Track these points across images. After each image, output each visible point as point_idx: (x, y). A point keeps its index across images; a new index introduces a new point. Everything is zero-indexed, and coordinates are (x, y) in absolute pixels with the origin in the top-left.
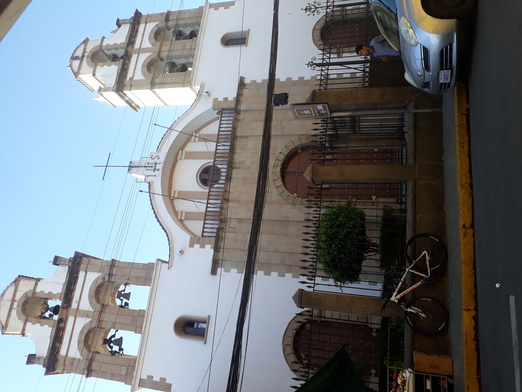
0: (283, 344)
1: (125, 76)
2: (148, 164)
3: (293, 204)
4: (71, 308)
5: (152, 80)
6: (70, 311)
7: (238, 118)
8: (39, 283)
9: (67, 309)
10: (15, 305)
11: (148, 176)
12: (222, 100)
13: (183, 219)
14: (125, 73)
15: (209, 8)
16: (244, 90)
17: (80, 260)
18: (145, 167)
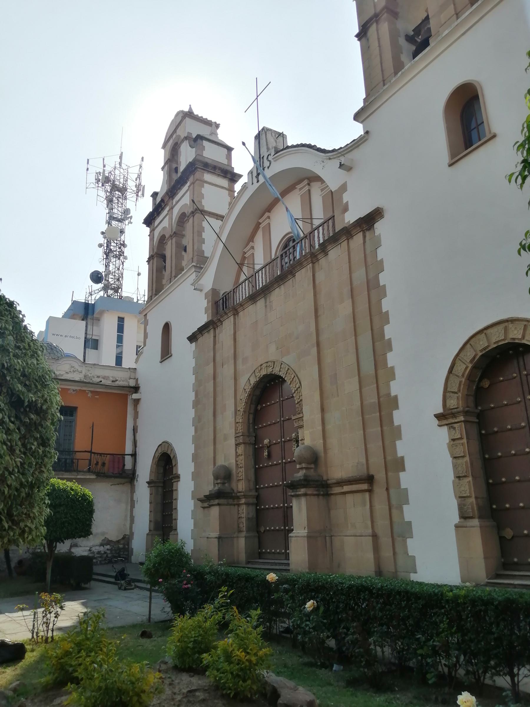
7: (319, 256)
9: (169, 198)
12: (345, 202)
13: (246, 255)
16: (361, 233)
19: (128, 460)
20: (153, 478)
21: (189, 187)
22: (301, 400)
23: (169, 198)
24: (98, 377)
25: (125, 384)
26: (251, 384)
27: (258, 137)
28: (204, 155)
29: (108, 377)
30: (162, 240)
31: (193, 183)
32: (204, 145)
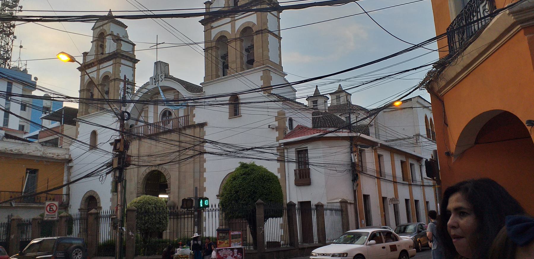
0: (90, 191)
1: (213, 21)
2: (158, 75)
3: (138, 183)
4: (100, 65)
5: (210, 48)
6: (98, 66)
8: (109, 36)
9: (98, 63)
10: (101, 28)
11: (152, 79)
12: (194, 113)
14: (215, 19)
15: (263, 71)
17: (117, 57)
18: (157, 74)
19: (65, 198)
20: (83, 207)
21: (112, 64)
22: (170, 183)
23: (98, 63)
24: (50, 153)
25: (63, 157)
26: (146, 173)
27: (156, 63)
28: (122, 49)
29: (55, 153)
30: (91, 82)
31: (115, 64)
32: (122, 43)
